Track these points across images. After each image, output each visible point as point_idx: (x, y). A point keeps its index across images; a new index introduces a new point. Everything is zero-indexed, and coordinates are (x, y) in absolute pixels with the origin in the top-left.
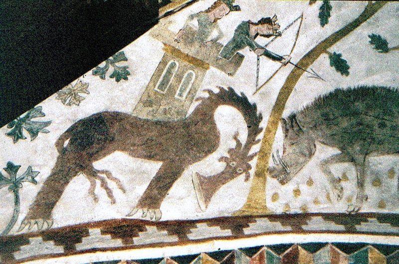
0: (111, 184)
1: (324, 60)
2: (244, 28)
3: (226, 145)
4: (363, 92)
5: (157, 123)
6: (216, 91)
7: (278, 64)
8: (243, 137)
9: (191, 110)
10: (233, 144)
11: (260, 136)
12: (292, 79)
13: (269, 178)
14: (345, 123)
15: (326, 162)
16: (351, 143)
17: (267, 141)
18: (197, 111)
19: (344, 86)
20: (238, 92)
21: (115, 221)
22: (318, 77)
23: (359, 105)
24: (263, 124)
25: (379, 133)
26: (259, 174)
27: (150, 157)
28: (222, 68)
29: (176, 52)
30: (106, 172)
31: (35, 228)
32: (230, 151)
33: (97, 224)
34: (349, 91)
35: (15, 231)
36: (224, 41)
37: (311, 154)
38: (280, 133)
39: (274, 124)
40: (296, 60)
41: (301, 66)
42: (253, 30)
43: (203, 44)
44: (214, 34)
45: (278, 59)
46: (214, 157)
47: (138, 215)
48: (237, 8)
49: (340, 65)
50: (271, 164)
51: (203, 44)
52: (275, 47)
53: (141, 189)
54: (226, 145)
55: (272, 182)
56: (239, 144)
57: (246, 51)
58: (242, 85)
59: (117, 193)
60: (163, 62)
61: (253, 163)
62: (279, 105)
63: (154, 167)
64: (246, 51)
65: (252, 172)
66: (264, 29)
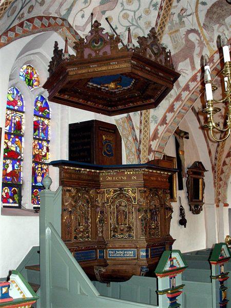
0: (185, 71)
1: (200, 5)
2: (179, 15)
3: (196, 43)
4: (214, 5)
5: (181, 50)
6: (185, 33)
7: (192, 16)
8: (198, 38)
9: (184, 42)
10: (197, 41)
11: (201, 35)
12: (197, 16)
13: (210, 43)
14: (215, 16)
15: (218, 29)
16: (219, 20)
17: (203, 35)
18: (185, 41)
19: (208, 8)
20: (189, 29)
21: (191, 78)
22: (201, 11)
23: (215, 10)
24: (200, 32)
25: (223, 13)
26: (207, 44)
27: (186, 59)
28: (182, 27)
29: (171, 33)
30: (181, 69)
31: (180, 91)
32: (198, 43)
33: (189, 81)
34: (210, 8)
35: (178, 94)
36: (178, 22)
37: (214, 30)
38: (204, 30)
39: (201, 29)
40: (194, 11)
41: (196, 11)
42: (181, 14)
43: (174, 26)
44: (175, 22)
45: (191, 14)
46: (196, 47)
47: (194, 73)
48: (174, 14)
49: (204, 4)
50: (208, 40)
51: (174, 26)
52: (188, 12)
53: (190, 68)
54: (196, 43)
55: (211, 43)
56: (198, 40)
57: (184, 19)
58: (188, 27)
59: (187, 72)
60: (170, 37)
61: (204, 42)
62: (199, 24)
63: (188, 60)
64: (184, 19)
65: (206, 44)
66: (183, 11)
